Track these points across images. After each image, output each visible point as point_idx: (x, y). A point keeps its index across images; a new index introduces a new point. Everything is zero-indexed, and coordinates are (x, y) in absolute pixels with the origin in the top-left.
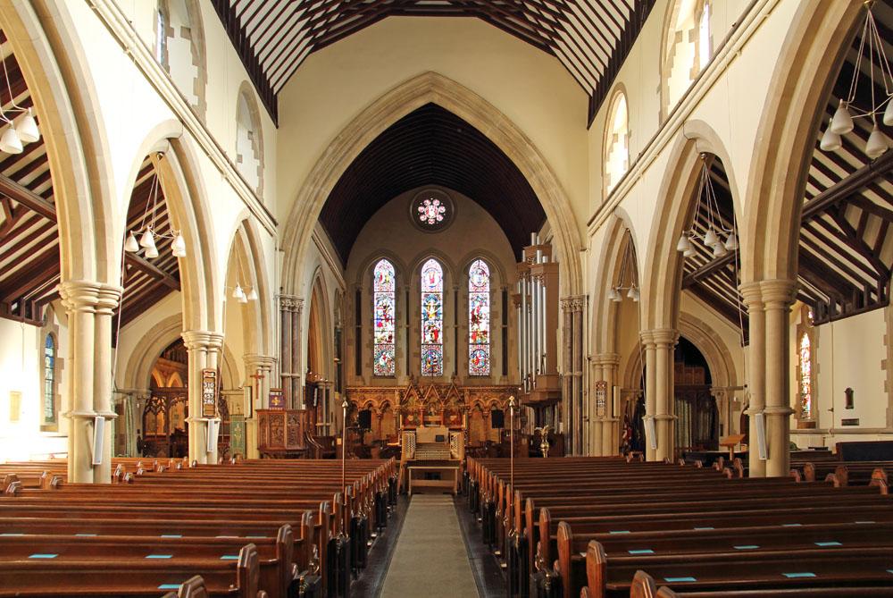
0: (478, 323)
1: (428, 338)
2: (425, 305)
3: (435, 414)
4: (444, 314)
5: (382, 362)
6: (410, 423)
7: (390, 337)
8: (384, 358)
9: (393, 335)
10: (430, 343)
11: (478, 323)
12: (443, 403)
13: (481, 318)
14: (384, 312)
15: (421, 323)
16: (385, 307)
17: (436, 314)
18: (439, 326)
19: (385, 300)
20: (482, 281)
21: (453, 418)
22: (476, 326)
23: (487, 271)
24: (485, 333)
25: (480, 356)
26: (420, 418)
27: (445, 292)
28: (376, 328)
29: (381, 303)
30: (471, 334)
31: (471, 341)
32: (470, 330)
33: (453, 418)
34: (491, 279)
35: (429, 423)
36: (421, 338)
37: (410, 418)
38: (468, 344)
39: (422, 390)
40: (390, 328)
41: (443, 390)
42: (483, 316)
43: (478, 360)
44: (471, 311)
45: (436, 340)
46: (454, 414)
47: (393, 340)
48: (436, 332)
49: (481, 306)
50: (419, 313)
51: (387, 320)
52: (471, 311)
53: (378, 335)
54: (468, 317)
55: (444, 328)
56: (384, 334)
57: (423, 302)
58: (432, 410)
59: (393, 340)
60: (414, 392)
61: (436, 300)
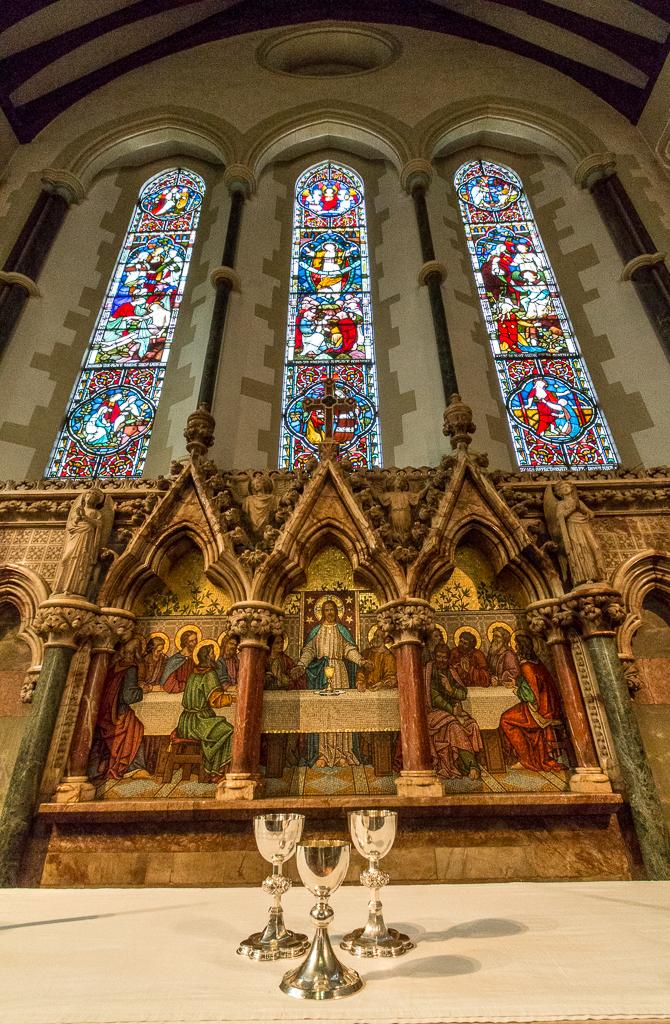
0: (516, 297)
1: (314, 342)
2: (303, 257)
3: (355, 676)
4: (377, 272)
5: (94, 430)
6: (152, 756)
7: (156, 346)
8: (111, 417)
9: (170, 338)
10: (325, 356)
11: (516, 297)
12: (403, 585)
13: (521, 282)
14: (149, 277)
15: (286, 303)
16: (155, 267)
17: (345, 278)
18: (357, 306)
19: (160, 250)
20: (503, 199)
21: (490, 704)
22: (507, 306)
23: (513, 176)
24: (549, 322)
25: (551, 397)
26: (233, 715)
27: (376, 221)
28: (104, 319)
29: (143, 256)
30: (492, 328)
31: (497, 348)
32: (487, 313)
33: (490, 704)
34: (530, 190)
35: (303, 749)
36: (283, 343)
37: (160, 711)
38: (490, 359)
39: (255, 505)
40: (161, 315)
41: (399, 501)
42: (528, 276)
43: (547, 418)
44: (476, 266)
45: (346, 348)
46: (485, 672)
47: (165, 355)
48: (348, 328)
49: (513, 252)
50: (277, 265)
51: (154, 297)
52: (476, 263)
53: (109, 338)
54: (473, 281)
55: (381, 307)
56: (133, 335)
57: (296, 249)
58: (327, 639)
59: (165, 355)
60: (199, 512)
61: (343, 244)
